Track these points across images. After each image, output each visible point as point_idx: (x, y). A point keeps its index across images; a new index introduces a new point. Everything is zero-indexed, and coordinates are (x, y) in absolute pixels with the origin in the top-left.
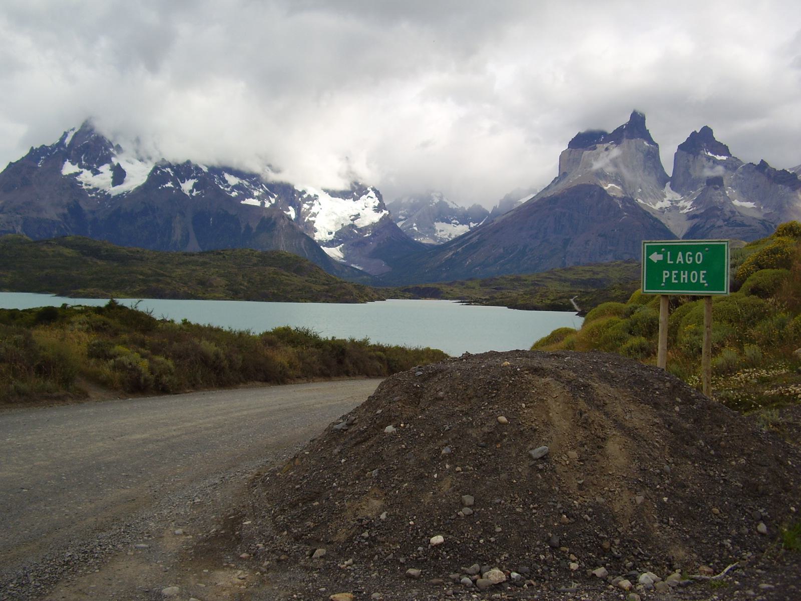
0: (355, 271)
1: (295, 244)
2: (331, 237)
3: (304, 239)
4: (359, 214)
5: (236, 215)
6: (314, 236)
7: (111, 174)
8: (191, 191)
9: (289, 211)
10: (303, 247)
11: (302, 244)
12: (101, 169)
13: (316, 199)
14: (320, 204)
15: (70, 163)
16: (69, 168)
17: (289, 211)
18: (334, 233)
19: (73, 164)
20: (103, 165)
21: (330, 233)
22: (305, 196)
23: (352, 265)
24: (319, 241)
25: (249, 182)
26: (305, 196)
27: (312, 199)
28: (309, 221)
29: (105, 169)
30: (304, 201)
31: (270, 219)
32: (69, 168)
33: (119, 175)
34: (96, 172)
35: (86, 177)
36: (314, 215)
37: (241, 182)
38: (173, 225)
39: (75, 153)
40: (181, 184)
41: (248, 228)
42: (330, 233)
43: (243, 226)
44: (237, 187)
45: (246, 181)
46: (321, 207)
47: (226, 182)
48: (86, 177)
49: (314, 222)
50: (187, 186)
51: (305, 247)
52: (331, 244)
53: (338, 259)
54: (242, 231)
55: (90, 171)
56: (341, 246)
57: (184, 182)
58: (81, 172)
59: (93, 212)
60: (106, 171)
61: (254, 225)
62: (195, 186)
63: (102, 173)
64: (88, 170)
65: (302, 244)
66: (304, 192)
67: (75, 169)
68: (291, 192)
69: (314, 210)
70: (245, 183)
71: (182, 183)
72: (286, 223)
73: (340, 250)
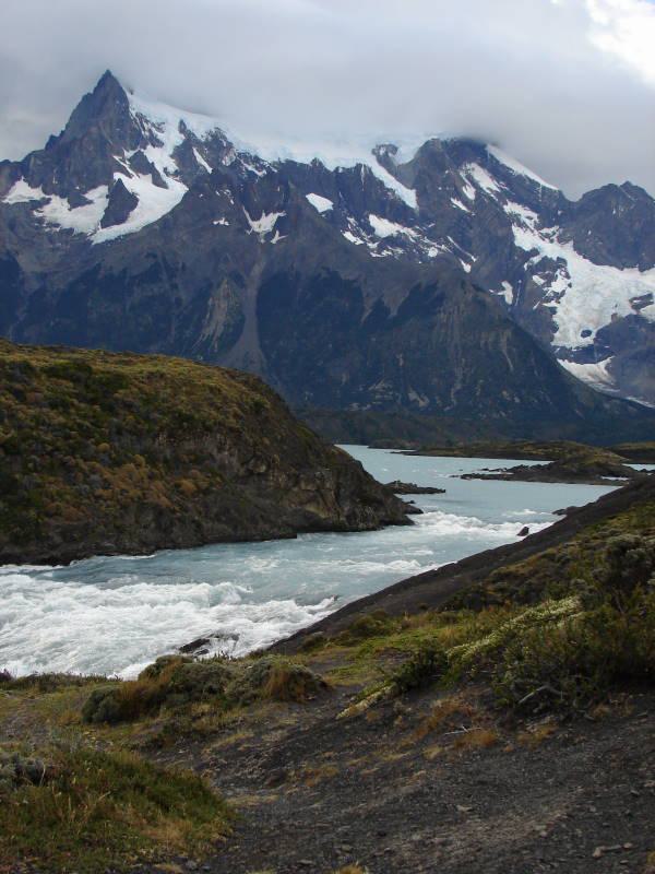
0: (630, 408)
1: (486, 344)
2: (589, 340)
3: (508, 333)
4: (650, 296)
5: (354, 281)
6: (552, 339)
7: (105, 203)
8: (270, 235)
9: (503, 289)
10: (504, 351)
11: (503, 340)
12: (90, 196)
13: (559, 267)
14: (568, 276)
15: (26, 184)
16: (22, 191)
17: (503, 289)
18: (593, 336)
19: (33, 185)
20: (94, 187)
21: (586, 333)
22: (536, 260)
23: (629, 398)
24: (563, 348)
25: (419, 232)
26: (536, 260)
27: (552, 267)
28: (541, 310)
29: (99, 196)
30: (534, 270)
31: (433, 287)
32: (22, 191)
33: (122, 203)
34: (77, 201)
35: (58, 211)
36: (558, 296)
37: (402, 231)
38: (210, 302)
39: (39, 162)
40: (250, 222)
41: (380, 308)
42: (586, 333)
43: (369, 305)
44: (390, 241)
45: (415, 230)
46: (569, 281)
47: (371, 230)
48: (58, 211)
49: (553, 311)
50: (265, 223)
51: (509, 352)
52: (585, 355)
53: (601, 387)
54: (366, 314)
55: (66, 200)
56: (608, 360)
57: (258, 219)
58: (48, 201)
59: (43, 276)
60: (99, 196)
61: (394, 300)
62: (279, 225)
63: (90, 202)
64: (62, 196)
65: (503, 340)
66: (535, 252)
67: (37, 194)
68: (506, 251)
69: (557, 286)
70: (411, 233)
71: (253, 219)
72: (470, 297)
73: (607, 368)
